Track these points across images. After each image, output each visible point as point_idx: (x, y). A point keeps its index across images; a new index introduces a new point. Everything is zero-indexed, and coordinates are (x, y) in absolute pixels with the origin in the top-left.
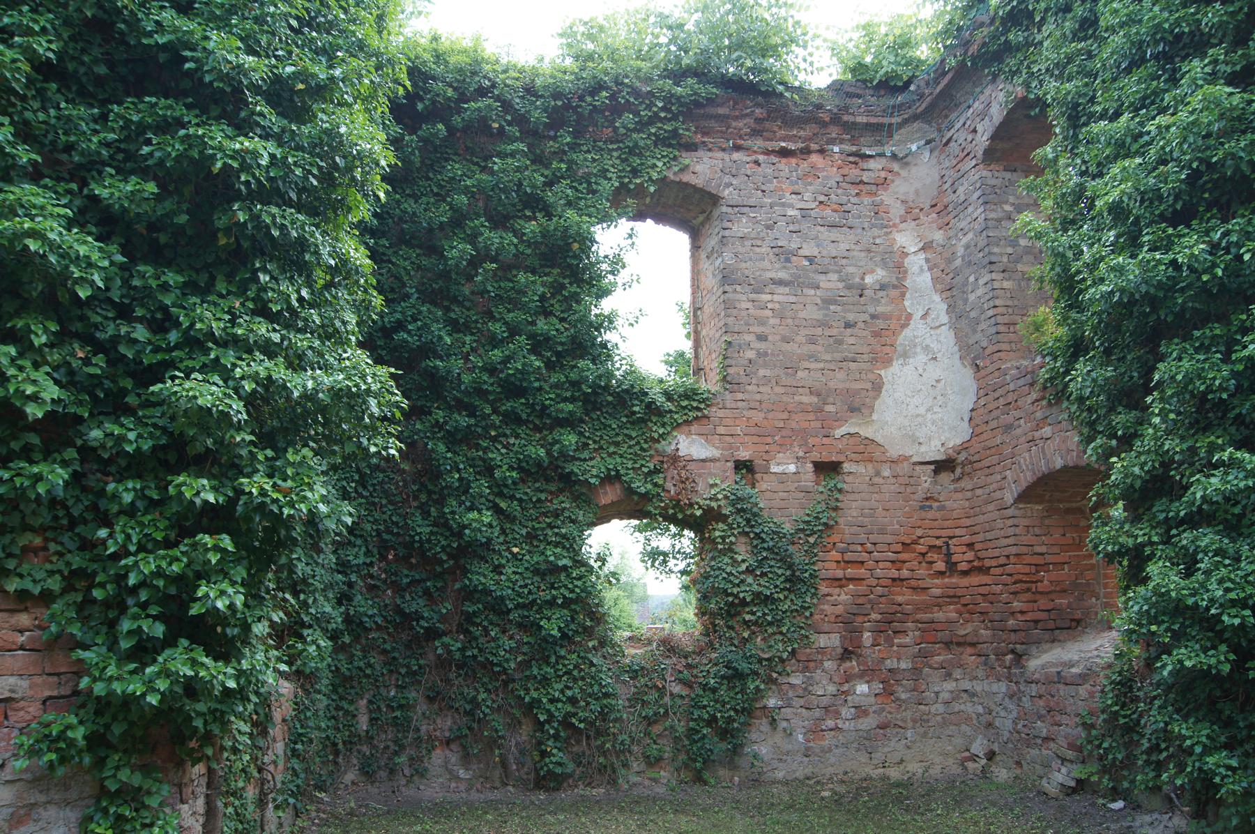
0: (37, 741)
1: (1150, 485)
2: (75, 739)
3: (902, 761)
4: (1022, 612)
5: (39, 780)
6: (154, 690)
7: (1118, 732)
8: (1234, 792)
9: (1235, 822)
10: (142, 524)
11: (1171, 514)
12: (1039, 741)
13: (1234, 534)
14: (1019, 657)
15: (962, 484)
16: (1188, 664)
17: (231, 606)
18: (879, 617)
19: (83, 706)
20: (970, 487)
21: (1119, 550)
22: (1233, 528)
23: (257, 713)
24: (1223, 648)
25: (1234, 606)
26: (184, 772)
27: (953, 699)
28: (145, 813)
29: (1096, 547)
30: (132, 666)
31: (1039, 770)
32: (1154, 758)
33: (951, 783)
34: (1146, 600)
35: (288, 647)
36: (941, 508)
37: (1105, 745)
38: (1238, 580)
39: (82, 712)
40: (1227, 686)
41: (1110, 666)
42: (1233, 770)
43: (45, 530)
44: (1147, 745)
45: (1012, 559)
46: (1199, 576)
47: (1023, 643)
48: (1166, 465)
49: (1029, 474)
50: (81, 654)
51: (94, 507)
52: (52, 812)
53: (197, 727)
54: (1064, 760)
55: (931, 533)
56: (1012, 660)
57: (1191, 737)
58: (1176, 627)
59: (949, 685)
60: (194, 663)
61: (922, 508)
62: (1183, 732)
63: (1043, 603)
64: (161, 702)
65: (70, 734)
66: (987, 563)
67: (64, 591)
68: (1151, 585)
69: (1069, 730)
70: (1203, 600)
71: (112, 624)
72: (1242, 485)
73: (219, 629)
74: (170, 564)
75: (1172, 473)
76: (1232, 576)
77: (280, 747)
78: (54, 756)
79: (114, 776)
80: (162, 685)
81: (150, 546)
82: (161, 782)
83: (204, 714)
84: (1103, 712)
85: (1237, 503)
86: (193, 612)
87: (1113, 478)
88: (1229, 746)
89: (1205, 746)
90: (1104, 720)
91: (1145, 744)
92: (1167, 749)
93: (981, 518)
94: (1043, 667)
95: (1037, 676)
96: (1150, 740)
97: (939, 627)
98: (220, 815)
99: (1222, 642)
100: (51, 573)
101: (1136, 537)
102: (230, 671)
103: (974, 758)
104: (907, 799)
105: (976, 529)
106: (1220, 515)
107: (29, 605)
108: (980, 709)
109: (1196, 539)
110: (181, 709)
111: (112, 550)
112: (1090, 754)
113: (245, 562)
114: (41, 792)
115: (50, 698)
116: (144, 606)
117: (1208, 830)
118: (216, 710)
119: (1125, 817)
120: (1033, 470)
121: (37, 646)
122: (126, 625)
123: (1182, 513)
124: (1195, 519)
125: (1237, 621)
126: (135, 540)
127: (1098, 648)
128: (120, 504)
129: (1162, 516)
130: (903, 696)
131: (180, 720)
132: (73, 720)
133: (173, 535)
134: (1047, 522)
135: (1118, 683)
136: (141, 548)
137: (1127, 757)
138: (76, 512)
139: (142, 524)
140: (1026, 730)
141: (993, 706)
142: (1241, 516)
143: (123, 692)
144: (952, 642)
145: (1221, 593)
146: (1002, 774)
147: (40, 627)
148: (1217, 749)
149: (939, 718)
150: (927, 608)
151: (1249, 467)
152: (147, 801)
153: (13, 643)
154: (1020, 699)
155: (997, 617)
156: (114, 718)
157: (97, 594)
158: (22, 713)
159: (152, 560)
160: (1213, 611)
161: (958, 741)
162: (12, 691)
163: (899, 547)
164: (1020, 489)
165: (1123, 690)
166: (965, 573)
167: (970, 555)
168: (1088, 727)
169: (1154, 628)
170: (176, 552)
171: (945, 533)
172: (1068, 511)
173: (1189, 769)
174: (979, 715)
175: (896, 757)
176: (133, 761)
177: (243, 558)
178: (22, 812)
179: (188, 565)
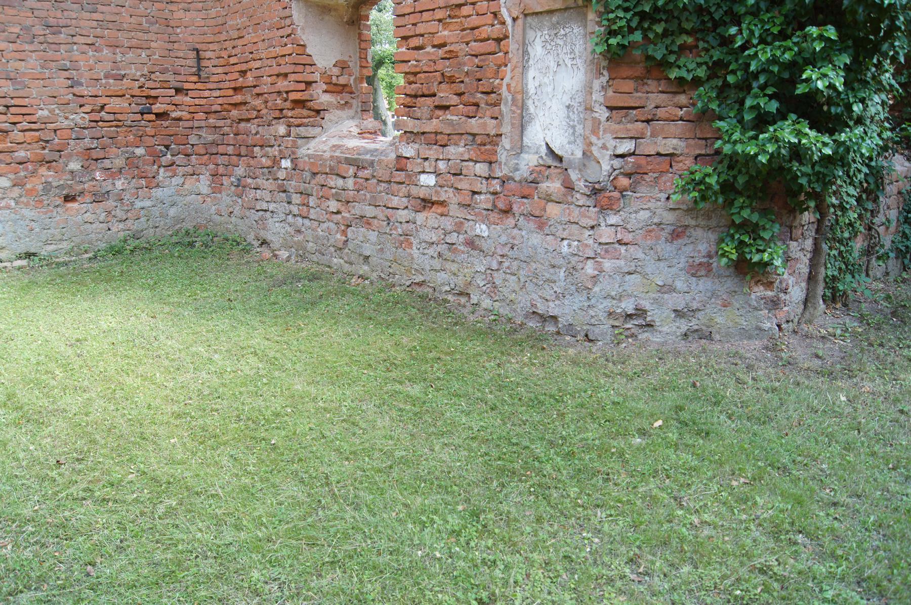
0: (687, 183)
2: (710, 185)
5: (692, 210)
6: (765, 152)
10: (762, 21)
17: (831, 86)
19: (721, 162)
23: (867, 182)
26: (795, 217)
28: (760, 242)
30: (752, 133)
35: (902, 130)
39: (720, 166)
43: (696, 32)
50: (720, 124)
51: (730, 12)
52: (699, 233)
53: (801, 185)
60: (799, 133)
64: (769, 161)
65: (707, 180)
67: (709, 78)
71: (742, 103)
73: (825, 108)
74: (783, 53)
77: (893, 214)
78: (697, 194)
79: (739, 213)
80: (771, 148)
81: (769, 39)
82: (773, 222)
83: (809, 175)
86: (798, 92)
98: (824, 255)
100: (699, 65)
102: (826, 139)
107: (686, 88)
110: (790, 169)
111: (739, 43)
113: (851, 51)
114: (692, 218)
115: (700, 155)
116: (763, 88)
118: (819, 172)
121: (691, 118)
122: (749, 103)
126: (757, 34)
128: (746, 6)
131: (788, 177)
132: (710, 170)
133: (789, 31)
136: (762, 41)
138: (717, 17)
139: (762, 21)
143: (743, 152)
147: (694, 105)
152: (762, 234)
153: (676, 115)
156: (740, 172)
157: (731, 79)
158: (681, 164)
159: (768, 50)
162: (675, 149)
170: (789, 43)
176: (754, 204)
177: (849, 47)
178: (680, 230)
179: (800, 52)
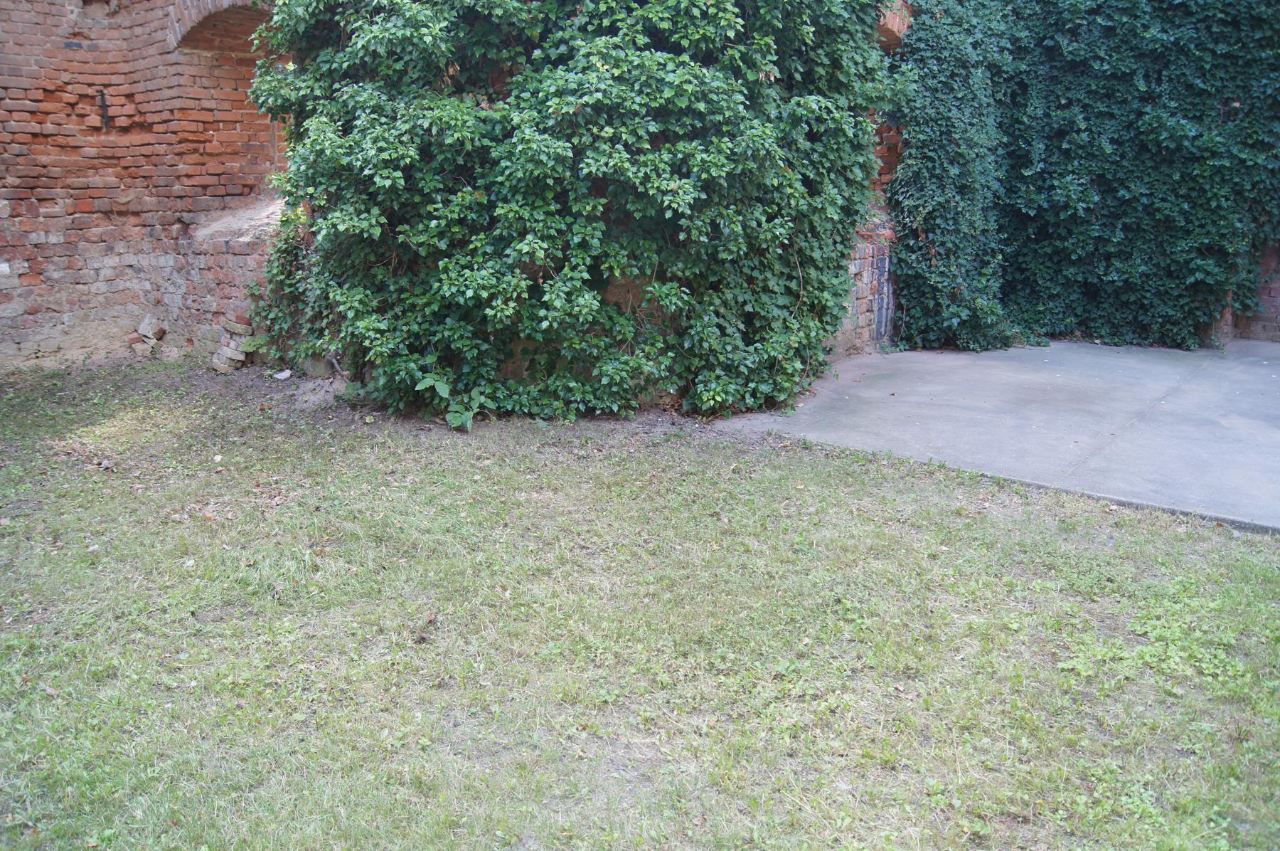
1: (317, 33)
3: (60, 349)
4: (188, 176)
7: (285, 302)
8: (381, 354)
9: (382, 381)
11: (335, 65)
12: (209, 316)
13: (394, 92)
14: (186, 226)
15: (118, 19)
16: (341, 228)
18: (18, 181)
20: (127, 24)
21: (282, 105)
22: (394, 86)
24: (375, 211)
25: (386, 168)
27: (117, 276)
29: (258, 97)
31: (211, 346)
32: (317, 326)
33: (116, 369)
34: (305, 159)
36: (94, 48)
37: (272, 316)
38: (392, 139)
40: (381, 250)
41: (278, 234)
42: (382, 332)
44: (310, 313)
45: (177, 115)
46: (355, 135)
47: (190, 211)
48: (331, 9)
49: (194, 12)
54: (232, 334)
55: (81, 78)
56: (179, 231)
57: (345, 303)
58: (332, 189)
59: (112, 261)
61: (68, 46)
62: (338, 298)
63: (213, 166)
66: (150, 118)
68: (307, 141)
69: (240, 303)
70: (358, 160)
72: (399, 34)
75: (337, 18)
76: (386, 135)
84: (270, 282)
85: (400, 59)
87: (276, 18)
88: (381, 310)
89: (357, 311)
90: (272, 291)
91: (309, 313)
92: (327, 316)
93: (141, 64)
94: (212, 236)
95: (205, 247)
96: (313, 308)
97: (96, 193)
99: (376, 204)
101: (300, 88)
103: (143, 339)
104: (61, 390)
105: (136, 77)
106: (383, 70)
108: (148, 286)
109: (358, 93)
112: (258, 327)
117: (362, 392)
119: (289, 386)
120: (198, 6)
123: (345, 65)
124: (355, 74)
125: (388, 183)
127: (267, 216)
129: (325, 68)
130: (56, 275)
134: (216, 73)
135: (284, 251)
137: (294, 325)
140: (196, 306)
141: (161, 282)
142: (404, 72)
144: (112, 212)
145: (373, 152)
146: (172, 353)
148: (369, 313)
149: (101, 298)
150: (80, 170)
151: (408, 15)
154: (188, 273)
155: (162, 181)
160: (367, 172)
161: (126, 322)
163: (39, 95)
164: (184, 30)
165: (289, 258)
166: (125, 130)
167: (130, 109)
168: (256, 298)
169: (311, 190)
171: (99, 80)
172: (241, 62)
173: (342, 335)
174: (147, 292)
175: (53, 344)
